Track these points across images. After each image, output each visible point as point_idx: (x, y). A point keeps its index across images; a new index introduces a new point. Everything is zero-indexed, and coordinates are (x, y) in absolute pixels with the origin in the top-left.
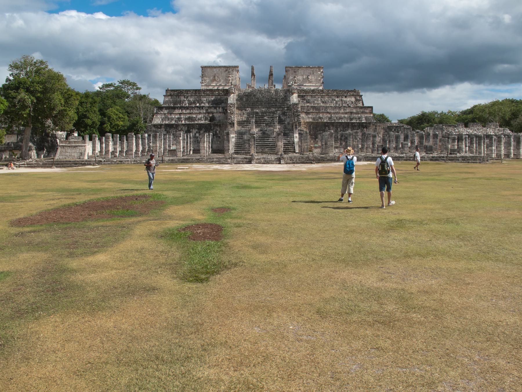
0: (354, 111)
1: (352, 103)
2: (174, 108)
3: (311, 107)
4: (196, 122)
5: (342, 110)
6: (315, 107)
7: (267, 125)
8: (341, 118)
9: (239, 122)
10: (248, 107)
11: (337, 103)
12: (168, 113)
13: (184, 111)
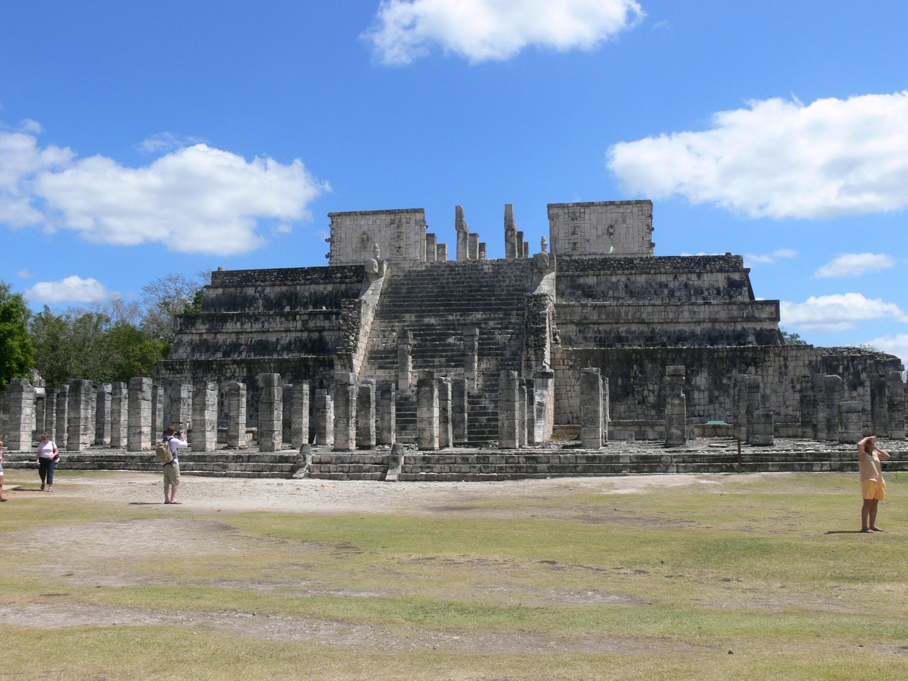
0: (723, 315)
1: (719, 293)
2: (224, 319)
3: (595, 307)
4: (275, 356)
5: (686, 314)
6: (605, 306)
7: (449, 360)
8: (681, 338)
9: (378, 352)
10: (407, 312)
11: (672, 293)
12: (209, 331)
13: (247, 326)
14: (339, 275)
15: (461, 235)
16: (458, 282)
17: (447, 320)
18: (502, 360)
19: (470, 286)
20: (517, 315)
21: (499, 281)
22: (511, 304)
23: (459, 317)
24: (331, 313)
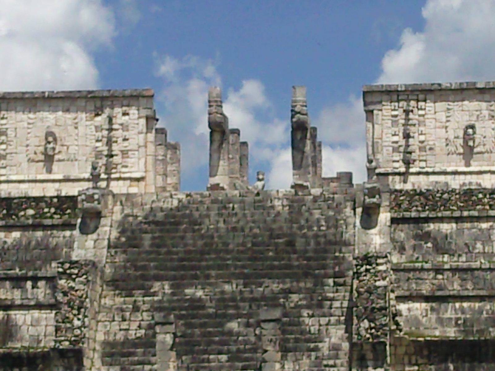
10: (158, 278)
14: (31, 212)
15: (217, 137)
16: (234, 229)
17: (223, 292)
18: (317, 358)
19: (255, 236)
20: (336, 284)
21: (301, 228)
22: (324, 267)
23: (241, 287)
24: (25, 279)
